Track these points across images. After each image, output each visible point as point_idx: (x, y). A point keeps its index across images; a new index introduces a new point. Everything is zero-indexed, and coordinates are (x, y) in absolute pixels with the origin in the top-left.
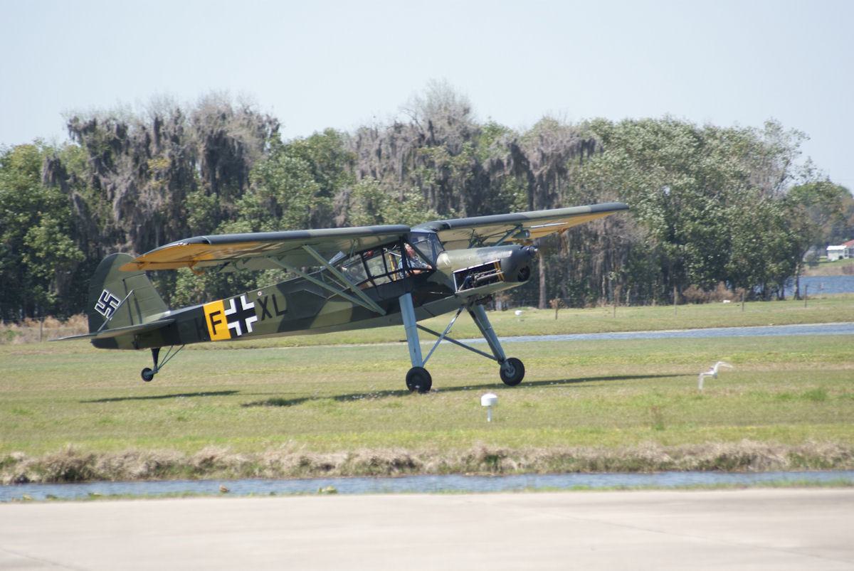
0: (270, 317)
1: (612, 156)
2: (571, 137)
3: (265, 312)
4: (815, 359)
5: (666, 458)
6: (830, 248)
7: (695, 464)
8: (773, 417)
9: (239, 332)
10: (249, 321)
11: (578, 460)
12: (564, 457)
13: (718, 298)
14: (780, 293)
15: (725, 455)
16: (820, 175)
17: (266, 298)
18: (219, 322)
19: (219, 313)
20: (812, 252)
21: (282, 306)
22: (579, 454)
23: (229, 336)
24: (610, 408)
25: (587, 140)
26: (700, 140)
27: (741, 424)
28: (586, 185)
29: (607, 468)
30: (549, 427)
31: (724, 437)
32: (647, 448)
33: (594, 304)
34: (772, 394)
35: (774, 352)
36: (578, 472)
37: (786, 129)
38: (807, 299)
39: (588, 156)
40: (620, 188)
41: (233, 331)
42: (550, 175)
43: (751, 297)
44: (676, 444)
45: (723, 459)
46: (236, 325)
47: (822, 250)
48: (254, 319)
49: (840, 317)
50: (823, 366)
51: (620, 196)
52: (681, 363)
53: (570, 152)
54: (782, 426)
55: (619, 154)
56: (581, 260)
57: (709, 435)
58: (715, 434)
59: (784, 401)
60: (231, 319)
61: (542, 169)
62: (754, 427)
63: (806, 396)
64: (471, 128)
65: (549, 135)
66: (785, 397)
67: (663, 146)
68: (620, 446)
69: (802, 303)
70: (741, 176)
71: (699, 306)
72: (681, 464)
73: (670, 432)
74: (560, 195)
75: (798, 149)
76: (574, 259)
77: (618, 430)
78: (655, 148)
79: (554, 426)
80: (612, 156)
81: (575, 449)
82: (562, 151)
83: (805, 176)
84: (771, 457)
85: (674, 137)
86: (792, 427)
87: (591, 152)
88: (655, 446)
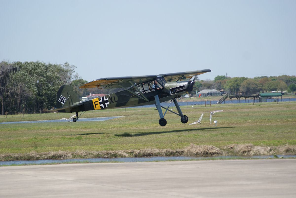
0: (113, 102)
1: (22, 72)
3: (111, 101)
5: (38, 156)
7: (46, 157)
8: (67, 144)
9: (103, 107)
10: (106, 104)
11: (13, 157)
12: (9, 156)
15: (54, 155)
16: (80, 78)
17: (112, 97)
18: (97, 104)
19: (97, 101)
21: (117, 99)
22: (13, 155)
23: (100, 109)
25: (15, 68)
26: (47, 68)
27: (58, 146)
28: (15, 80)
29: (21, 159)
30: (5, 148)
31: (54, 150)
32: (33, 153)
35: (68, 126)
36: (13, 160)
37: (70, 65)
39: (15, 72)
40: (24, 81)
41: (101, 107)
42: (4, 77)
44: (40, 152)
45: (54, 156)
46: (102, 105)
48: (108, 103)
49: (85, 116)
51: (24, 83)
52: (42, 130)
53: (10, 71)
54: (70, 147)
55: (24, 72)
56: (14, 101)
57: (50, 149)
58: (51, 149)
59: (70, 140)
60: (101, 103)
61: (2, 76)
65: (4, 66)
67: (37, 69)
68: (25, 153)
70: (58, 78)
72: (42, 158)
73: (39, 149)
74: (7, 83)
75: (74, 71)
76: (12, 101)
77: (24, 148)
78: (35, 70)
79: (6, 148)
80: (22, 72)
81: (12, 154)
82: (8, 71)
83: (76, 78)
84: (67, 155)
85: (40, 67)
86: (73, 147)
87: (16, 71)
88: (35, 153)
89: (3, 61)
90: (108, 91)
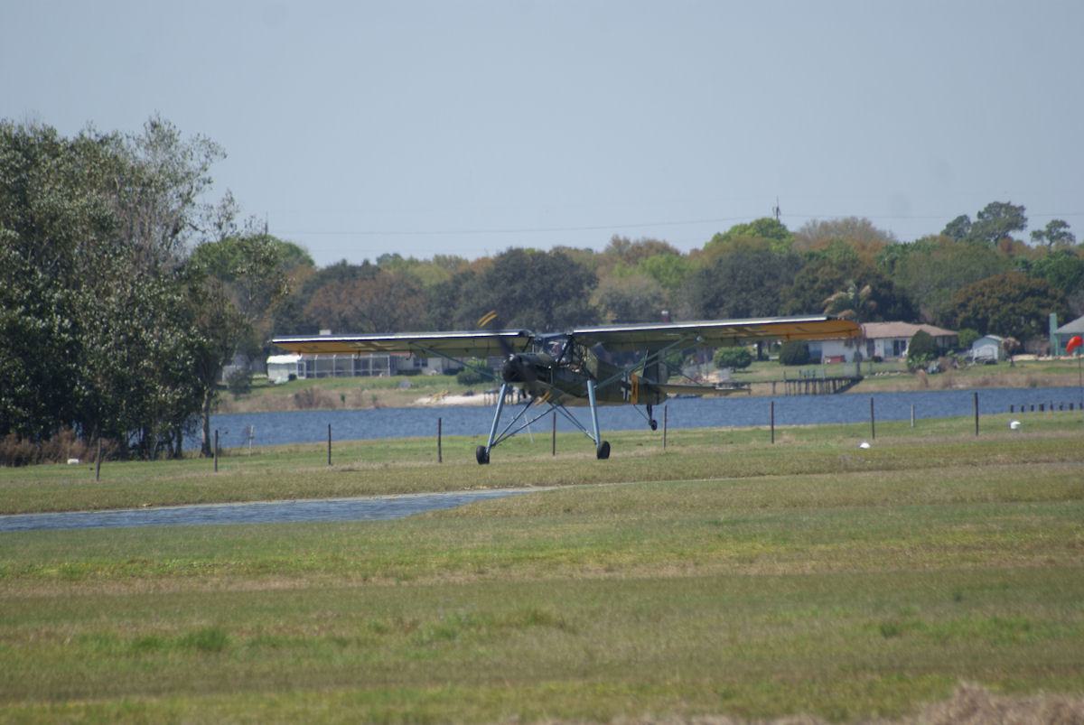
4: (216, 571)
6: (272, 359)
13: (58, 456)
14: (175, 444)
20: (239, 367)
35: (142, 558)
37: (184, 139)
38: (220, 453)
43: (123, 454)
47: (257, 363)
62: (82, 704)
63: (186, 644)
66: (149, 644)
69: (210, 463)
71: (20, 471)
75: (204, 175)
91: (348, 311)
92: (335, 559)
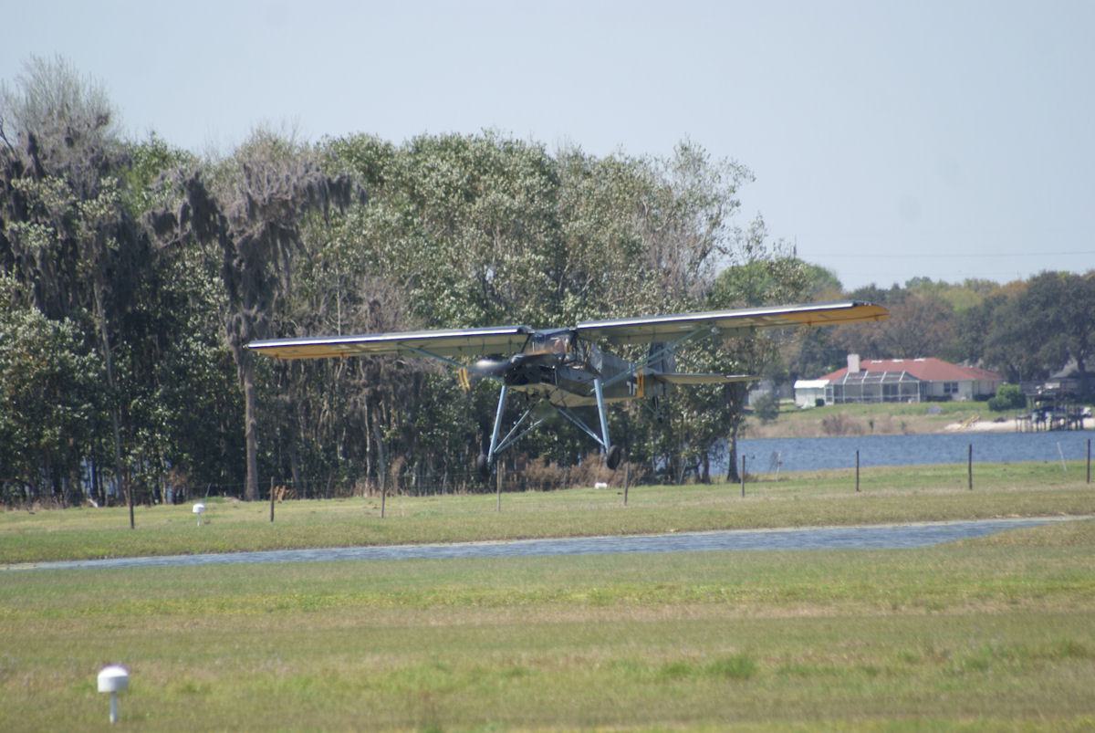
1: (381, 211)
2: (307, 171)
4: (744, 597)
6: (799, 384)
13: (586, 479)
14: (701, 469)
20: (766, 392)
24: (348, 694)
33: (348, 490)
34: (654, 666)
35: (670, 584)
37: (712, 162)
38: (747, 478)
43: (649, 480)
47: (785, 388)
49: (800, 516)
50: (759, 610)
52: (494, 606)
59: (675, 678)
63: (713, 671)
64: (112, 150)
66: (677, 671)
69: (737, 488)
75: (734, 197)
87: (345, 201)
89: (260, 133)
90: (975, 340)
91: (877, 335)
92: (864, 587)
